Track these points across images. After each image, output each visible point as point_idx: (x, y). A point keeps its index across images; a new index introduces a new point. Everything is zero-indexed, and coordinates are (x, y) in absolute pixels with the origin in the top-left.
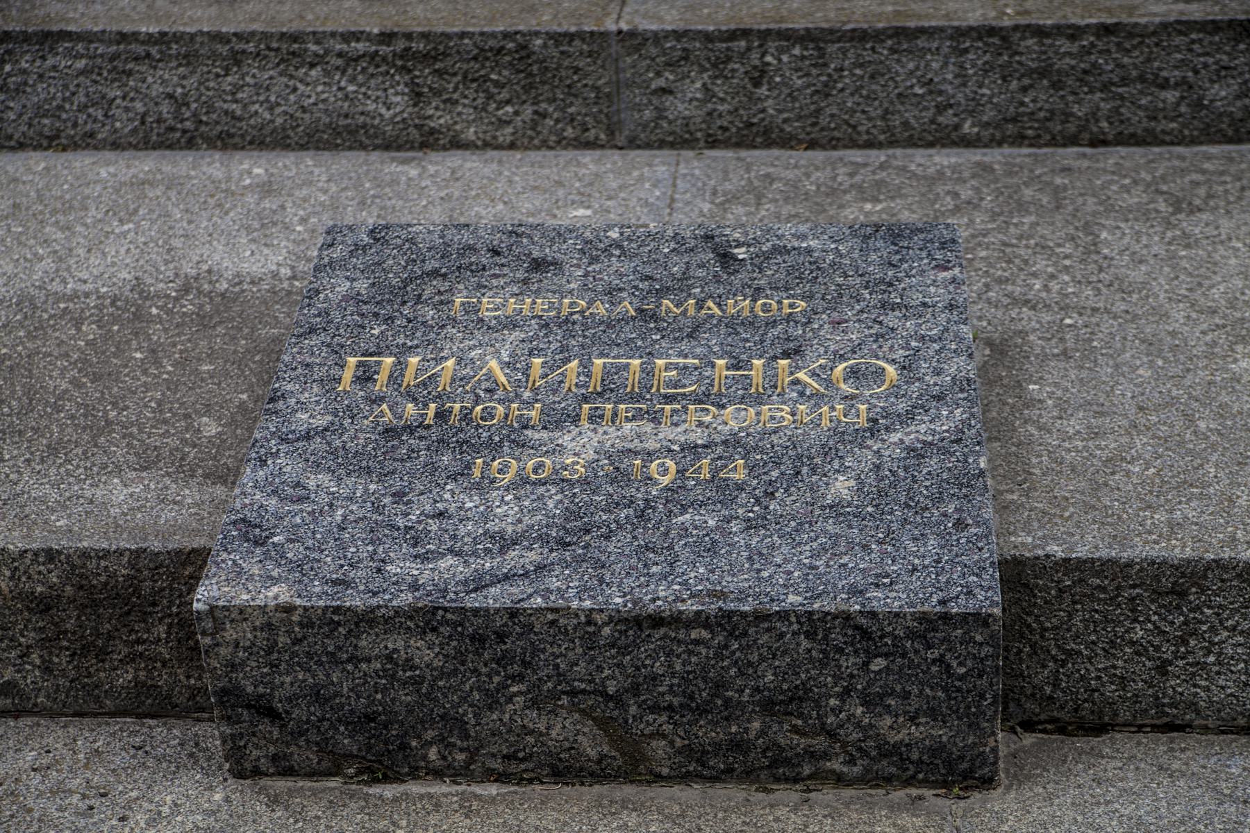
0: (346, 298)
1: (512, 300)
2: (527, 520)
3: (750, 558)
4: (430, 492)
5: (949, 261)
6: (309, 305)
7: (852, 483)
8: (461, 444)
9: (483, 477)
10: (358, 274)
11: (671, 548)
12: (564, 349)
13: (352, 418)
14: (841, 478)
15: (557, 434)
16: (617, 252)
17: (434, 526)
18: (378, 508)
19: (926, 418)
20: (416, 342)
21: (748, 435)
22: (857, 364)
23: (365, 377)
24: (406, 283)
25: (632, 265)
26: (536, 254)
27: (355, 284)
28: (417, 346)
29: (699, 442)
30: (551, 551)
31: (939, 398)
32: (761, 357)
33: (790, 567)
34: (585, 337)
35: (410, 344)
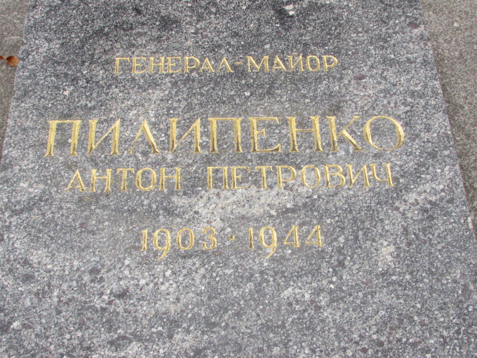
0: (47, 59)
1: (152, 58)
2: (184, 300)
3: (336, 336)
4: (115, 268)
5: (416, 19)
6: (23, 67)
7: (392, 248)
8: (132, 211)
9: (149, 250)
10: (53, 36)
11: (283, 326)
12: (190, 108)
13: (57, 186)
14: (385, 243)
15: (194, 200)
16: (213, 10)
17: (120, 305)
18: (82, 288)
19: (429, 177)
20: (93, 103)
21: (319, 197)
22: (378, 120)
23: (62, 143)
24: (84, 41)
25: (225, 22)
26: (163, 13)
27: (52, 45)
28: (94, 108)
29: (289, 206)
30: (203, 333)
31: (433, 155)
32: (316, 113)
33: (364, 344)
34: (202, 95)
35: (89, 105)
